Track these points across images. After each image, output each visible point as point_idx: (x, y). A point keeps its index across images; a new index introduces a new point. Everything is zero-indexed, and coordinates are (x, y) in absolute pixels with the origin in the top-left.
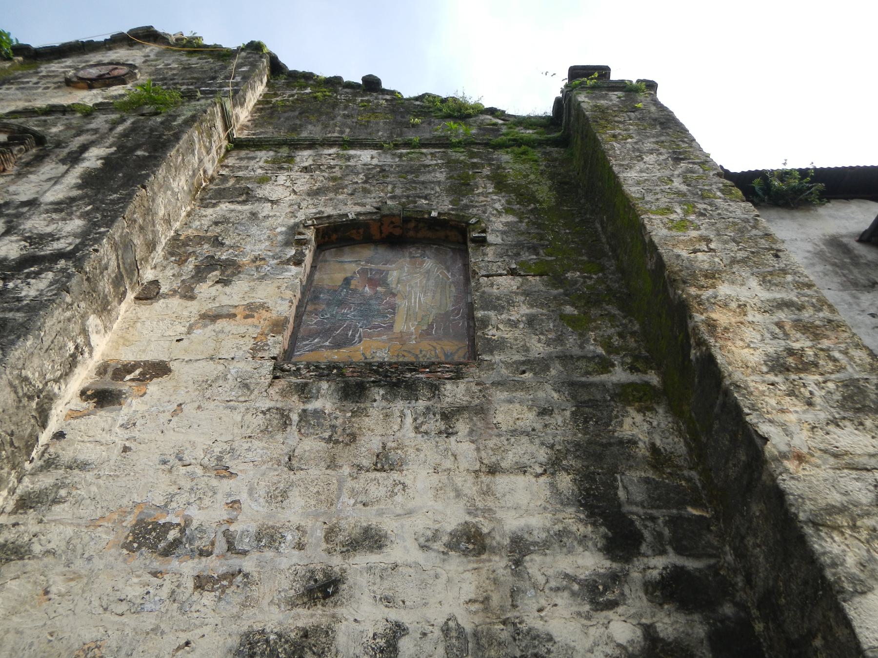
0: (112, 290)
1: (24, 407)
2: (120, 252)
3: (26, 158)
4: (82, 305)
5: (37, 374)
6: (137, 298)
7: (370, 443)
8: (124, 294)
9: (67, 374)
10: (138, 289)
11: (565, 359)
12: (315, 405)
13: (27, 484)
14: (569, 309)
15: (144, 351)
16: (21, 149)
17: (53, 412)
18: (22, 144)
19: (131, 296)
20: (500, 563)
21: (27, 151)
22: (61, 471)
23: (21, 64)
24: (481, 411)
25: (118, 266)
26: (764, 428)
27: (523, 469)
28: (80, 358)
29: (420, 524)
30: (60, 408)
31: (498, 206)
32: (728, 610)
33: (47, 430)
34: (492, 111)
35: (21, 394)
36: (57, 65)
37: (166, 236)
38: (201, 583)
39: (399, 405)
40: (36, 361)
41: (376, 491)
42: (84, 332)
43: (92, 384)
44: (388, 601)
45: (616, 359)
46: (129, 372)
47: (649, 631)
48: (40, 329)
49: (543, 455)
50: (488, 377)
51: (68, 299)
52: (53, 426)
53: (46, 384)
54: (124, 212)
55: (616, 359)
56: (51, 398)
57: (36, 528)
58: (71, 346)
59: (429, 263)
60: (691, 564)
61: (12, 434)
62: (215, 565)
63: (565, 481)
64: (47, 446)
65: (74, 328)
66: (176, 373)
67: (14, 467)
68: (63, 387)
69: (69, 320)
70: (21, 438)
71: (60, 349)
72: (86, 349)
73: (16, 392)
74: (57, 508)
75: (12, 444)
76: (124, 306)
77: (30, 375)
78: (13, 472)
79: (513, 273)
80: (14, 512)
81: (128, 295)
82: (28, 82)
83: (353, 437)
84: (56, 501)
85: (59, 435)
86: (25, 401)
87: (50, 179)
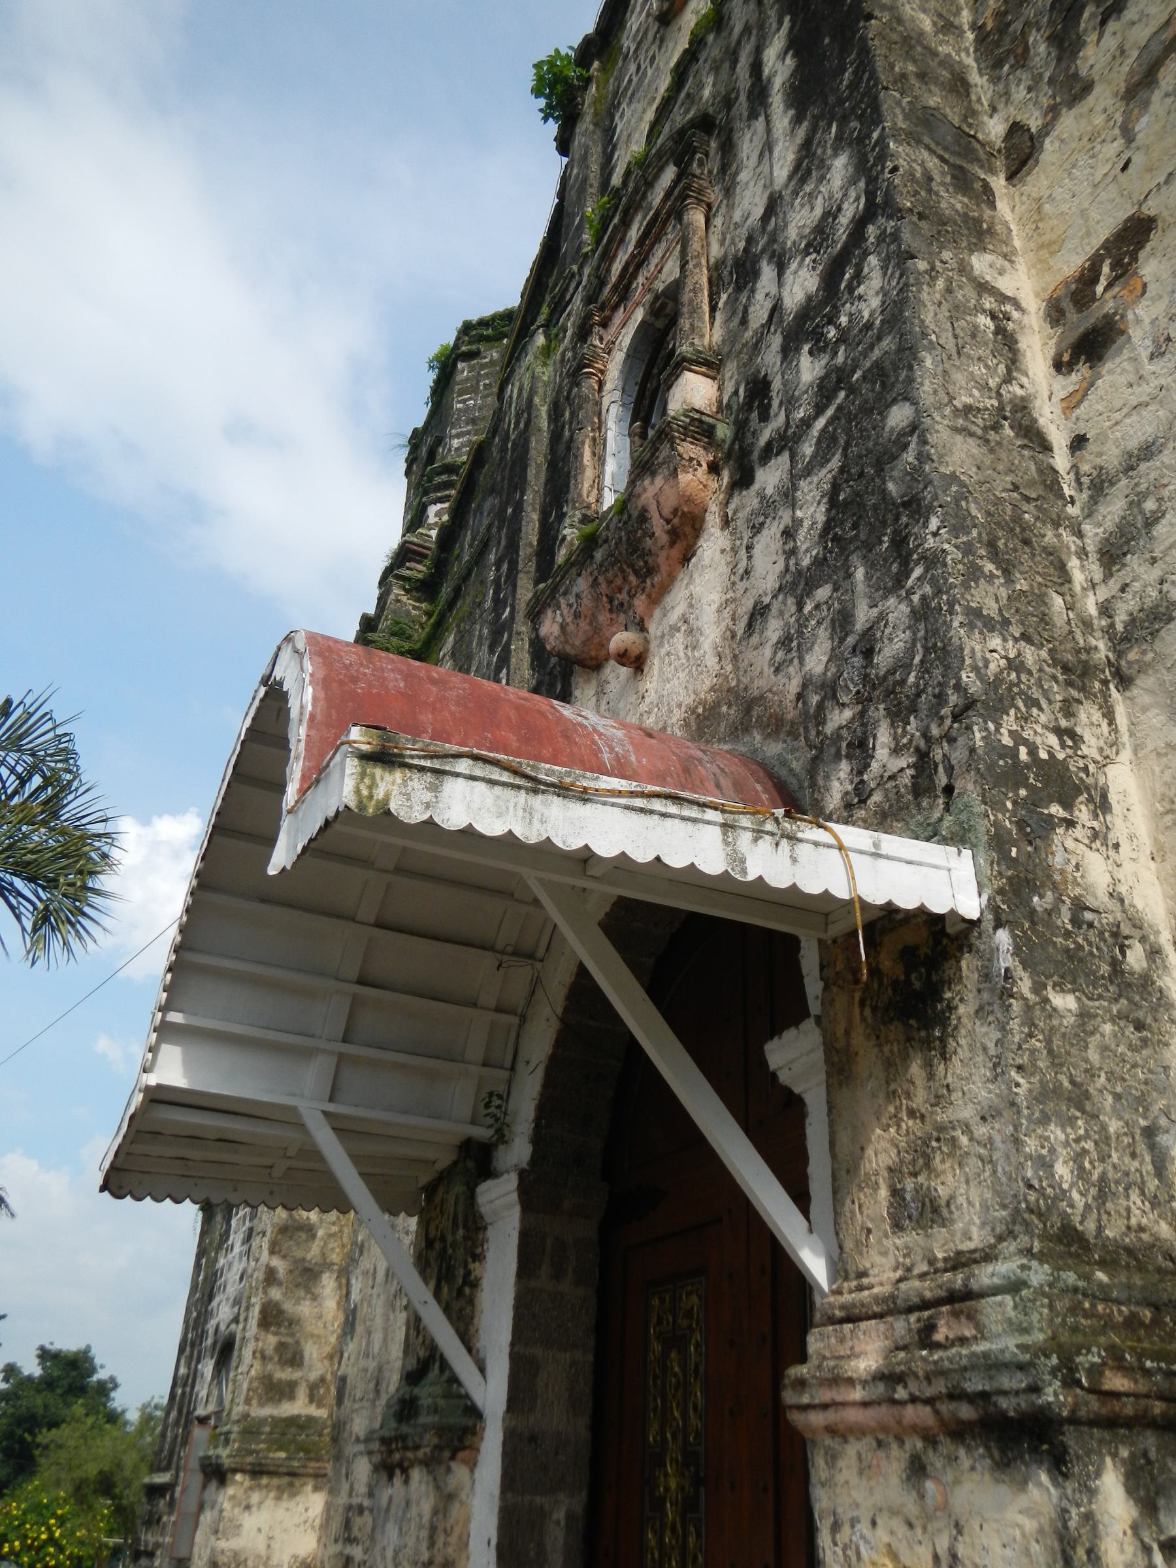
0: (966, 200)
1: (999, 443)
2: (927, 140)
3: (714, 164)
4: (946, 255)
5: (976, 392)
6: (1010, 178)
8: (987, 189)
9: (1014, 361)
10: (999, 163)
13: (1093, 533)
15: (1088, 234)
16: (700, 160)
17: (1042, 421)
18: (694, 153)
19: (998, 183)
21: (707, 155)
22: (1124, 482)
23: (603, 69)
25: (943, 160)
28: (1010, 326)
30: (1046, 410)
33: (1056, 449)
35: (979, 432)
36: (633, 18)
37: (967, 50)
40: (959, 378)
42: (983, 288)
43: (1058, 344)
46: (1095, 281)
48: (924, 335)
51: (922, 265)
52: (1059, 439)
53: (999, 395)
54: (877, 81)
56: (1022, 407)
57: (1156, 573)
58: (984, 321)
61: (1016, 487)
64: (1075, 468)
65: (965, 294)
66: (1165, 213)
67: (1056, 524)
68: (1024, 380)
69: (949, 290)
70: (1031, 484)
71: (974, 336)
72: (1008, 308)
73: (972, 435)
74: (1160, 530)
75: (1027, 499)
76: (1002, 206)
77: (969, 401)
78: (1061, 530)
80: (1108, 576)
81: (993, 185)
82: (630, 80)
84: (1151, 522)
85: (1078, 443)
86: (992, 435)
87: (761, 155)
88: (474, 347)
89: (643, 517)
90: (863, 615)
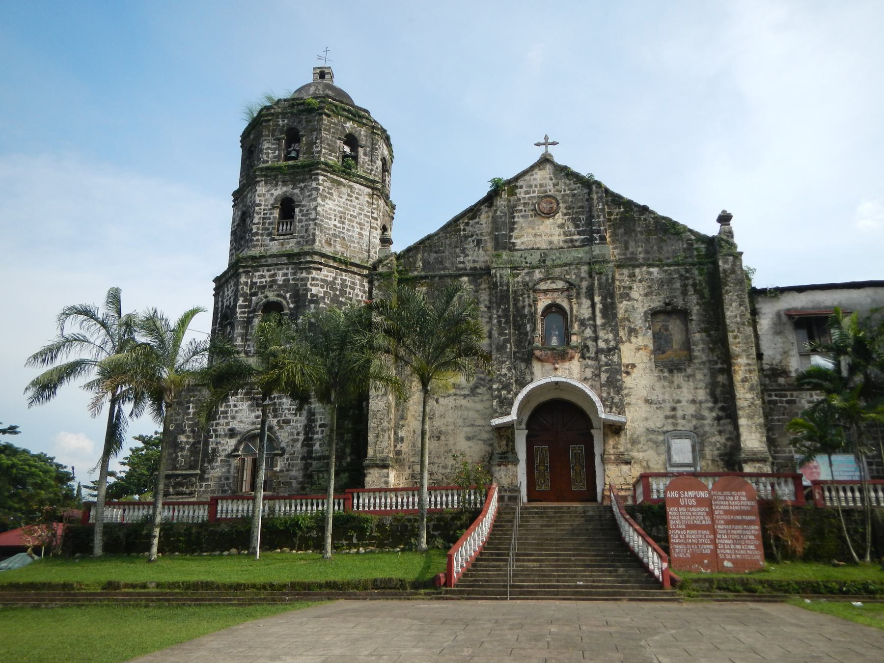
7: (676, 383)
11: (710, 361)
12: (665, 374)
14: (711, 346)
20: (698, 405)
24: (692, 376)
26: (737, 394)
27: (701, 388)
29: (686, 399)
31: (695, 301)
32: (729, 412)
34: (691, 231)
38: (657, 408)
39: (679, 374)
41: (679, 393)
44: (683, 411)
45: (719, 361)
47: (718, 415)
49: (704, 385)
50: (695, 367)
55: (719, 361)
59: (678, 322)
60: (725, 405)
62: (658, 406)
63: (708, 390)
79: (699, 332)
83: (673, 382)
88: (331, 113)
89: (567, 353)
90: (612, 395)
